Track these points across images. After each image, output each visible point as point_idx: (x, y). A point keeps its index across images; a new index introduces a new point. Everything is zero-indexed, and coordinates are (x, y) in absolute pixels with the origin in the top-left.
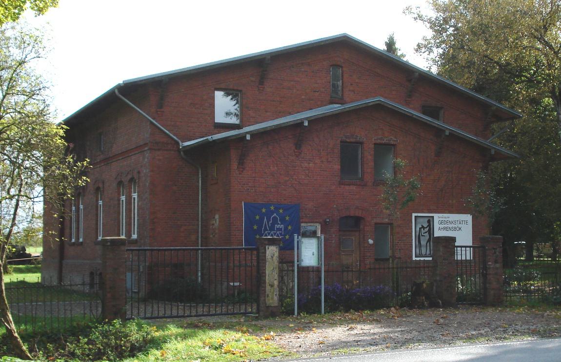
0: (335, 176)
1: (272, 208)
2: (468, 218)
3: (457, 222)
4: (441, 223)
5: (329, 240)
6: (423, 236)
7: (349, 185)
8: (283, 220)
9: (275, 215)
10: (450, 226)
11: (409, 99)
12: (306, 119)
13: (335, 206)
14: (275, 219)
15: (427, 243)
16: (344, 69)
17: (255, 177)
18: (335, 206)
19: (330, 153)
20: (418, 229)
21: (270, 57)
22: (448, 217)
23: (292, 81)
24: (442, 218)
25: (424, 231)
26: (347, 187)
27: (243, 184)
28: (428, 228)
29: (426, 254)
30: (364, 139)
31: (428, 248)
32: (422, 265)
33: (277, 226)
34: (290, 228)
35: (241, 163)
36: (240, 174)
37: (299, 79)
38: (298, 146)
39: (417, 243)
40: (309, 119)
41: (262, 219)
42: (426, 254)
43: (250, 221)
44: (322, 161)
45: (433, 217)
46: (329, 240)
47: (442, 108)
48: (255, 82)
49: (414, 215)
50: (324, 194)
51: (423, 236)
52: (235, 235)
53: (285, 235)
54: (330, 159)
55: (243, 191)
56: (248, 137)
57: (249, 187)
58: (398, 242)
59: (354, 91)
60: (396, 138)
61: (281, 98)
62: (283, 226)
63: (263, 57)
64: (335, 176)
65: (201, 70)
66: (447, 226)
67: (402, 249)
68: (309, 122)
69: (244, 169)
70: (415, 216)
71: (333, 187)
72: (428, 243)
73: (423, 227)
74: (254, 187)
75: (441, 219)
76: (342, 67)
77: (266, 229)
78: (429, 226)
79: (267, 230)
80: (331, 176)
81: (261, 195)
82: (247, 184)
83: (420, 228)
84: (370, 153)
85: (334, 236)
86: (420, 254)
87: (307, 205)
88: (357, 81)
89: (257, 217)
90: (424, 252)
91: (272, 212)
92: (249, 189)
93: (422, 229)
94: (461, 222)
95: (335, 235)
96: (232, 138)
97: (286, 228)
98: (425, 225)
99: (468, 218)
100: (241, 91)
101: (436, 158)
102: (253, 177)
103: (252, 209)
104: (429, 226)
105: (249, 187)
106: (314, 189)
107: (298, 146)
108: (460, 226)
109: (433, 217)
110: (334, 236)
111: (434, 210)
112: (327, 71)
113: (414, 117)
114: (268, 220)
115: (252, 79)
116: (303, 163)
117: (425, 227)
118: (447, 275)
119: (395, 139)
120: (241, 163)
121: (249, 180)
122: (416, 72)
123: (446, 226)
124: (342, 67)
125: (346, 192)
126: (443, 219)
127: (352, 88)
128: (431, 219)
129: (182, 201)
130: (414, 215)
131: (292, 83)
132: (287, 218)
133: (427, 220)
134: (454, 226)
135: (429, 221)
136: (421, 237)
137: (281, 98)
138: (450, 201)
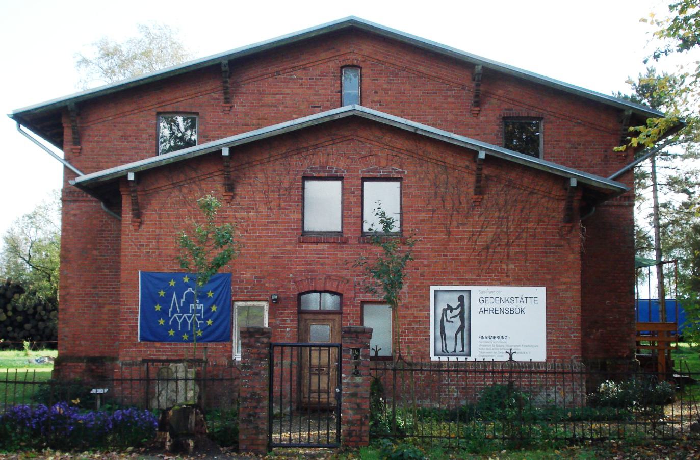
0: (293, 230)
1: (186, 280)
2: (540, 292)
3: (515, 300)
4: (485, 301)
5: (281, 328)
6: (449, 322)
7: (317, 243)
8: (203, 297)
9: (190, 289)
10: (503, 306)
11: (477, 109)
12: (226, 145)
13: (291, 276)
14: (190, 295)
15: (456, 335)
16: (364, 71)
17: (159, 235)
18: (291, 276)
19: (284, 195)
20: (440, 312)
21: (227, 62)
22: (499, 292)
23: (277, 94)
24: (487, 292)
25: (452, 315)
26: (313, 247)
27: (140, 245)
28: (459, 309)
29: (455, 351)
30: (343, 172)
31: (459, 341)
32: (481, 368)
33: (192, 306)
34: (214, 308)
35: (138, 214)
36: (136, 230)
37: (288, 91)
38: (230, 187)
39: (439, 333)
40: (231, 146)
41: (169, 296)
42: (455, 351)
43: (149, 298)
44: (270, 208)
45: (469, 292)
46: (281, 328)
47: (540, 119)
48: (218, 99)
49: (433, 288)
50: (274, 257)
51: (449, 322)
52: (127, 319)
53: (206, 319)
54: (283, 205)
55: (140, 256)
56: (131, 177)
57: (150, 249)
58: (405, 332)
59: (380, 102)
60: (401, 167)
61: (259, 119)
62: (203, 305)
63: (217, 62)
64: (293, 230)
65: (123, 88)
66: (497, 305)
67: (411, 342)
68: (231, 150)
69: (141, 223)
70: (470, 291)
71: (289, 247)
72: (459, 335)
73: (450, 308)
74: (158, 249)
75: (484, 295)
76: (361, 68)
77: (174, 311)
78: (462, 305)
79: (177, 312)
80: (286, 230)
81: (168, 260)
82: (147, 245)
83: (444, 310)
84: (354, 193)
85: (288, 321)
86: (443, 351)
87: (243, 274)
88: (385, 86)
89: (162, 293)
90: (450, 347)
91: (187, 286)
92: (149, 252)
93: (448, 311)
94: (525, 300)
95: (291, 321)
96: (102, 180)
97: (208, 310)
98: (455, 303)
99: (540, 292)
100: (197, 114)
101: (476, 197)
102: (156, 235)
103: (153, 281)
104: (462, 305)
105: (150, 249)
106: (256, 250)
107: (230, 187)
108: (521, 305)
109: (469, 292)
110: (288, 321)
111: (471, 280)
112: (335, 76)
113: (419, 132)
114: (179, 297)
115: (215, 95)
116: (238, 212)
117: (454, 307)
118: (248, 396)
119: (401, 170)
120: (138, 214)
121: (150, 239)
122: (478, 65)
123: (494, 305)
124: (361, 68)
125: (311, 254)
126: (489, 295)
127: (376, 99)
128: (466, 295)
129: (106, 270)
130: (433, 288)
131: (277, 97)
132: (210, 294)
133: (458, 295)
134: (510, 306)
135: (461, 299)
136: (446, 324)
137: (259, 119)
138: (504, 266)
